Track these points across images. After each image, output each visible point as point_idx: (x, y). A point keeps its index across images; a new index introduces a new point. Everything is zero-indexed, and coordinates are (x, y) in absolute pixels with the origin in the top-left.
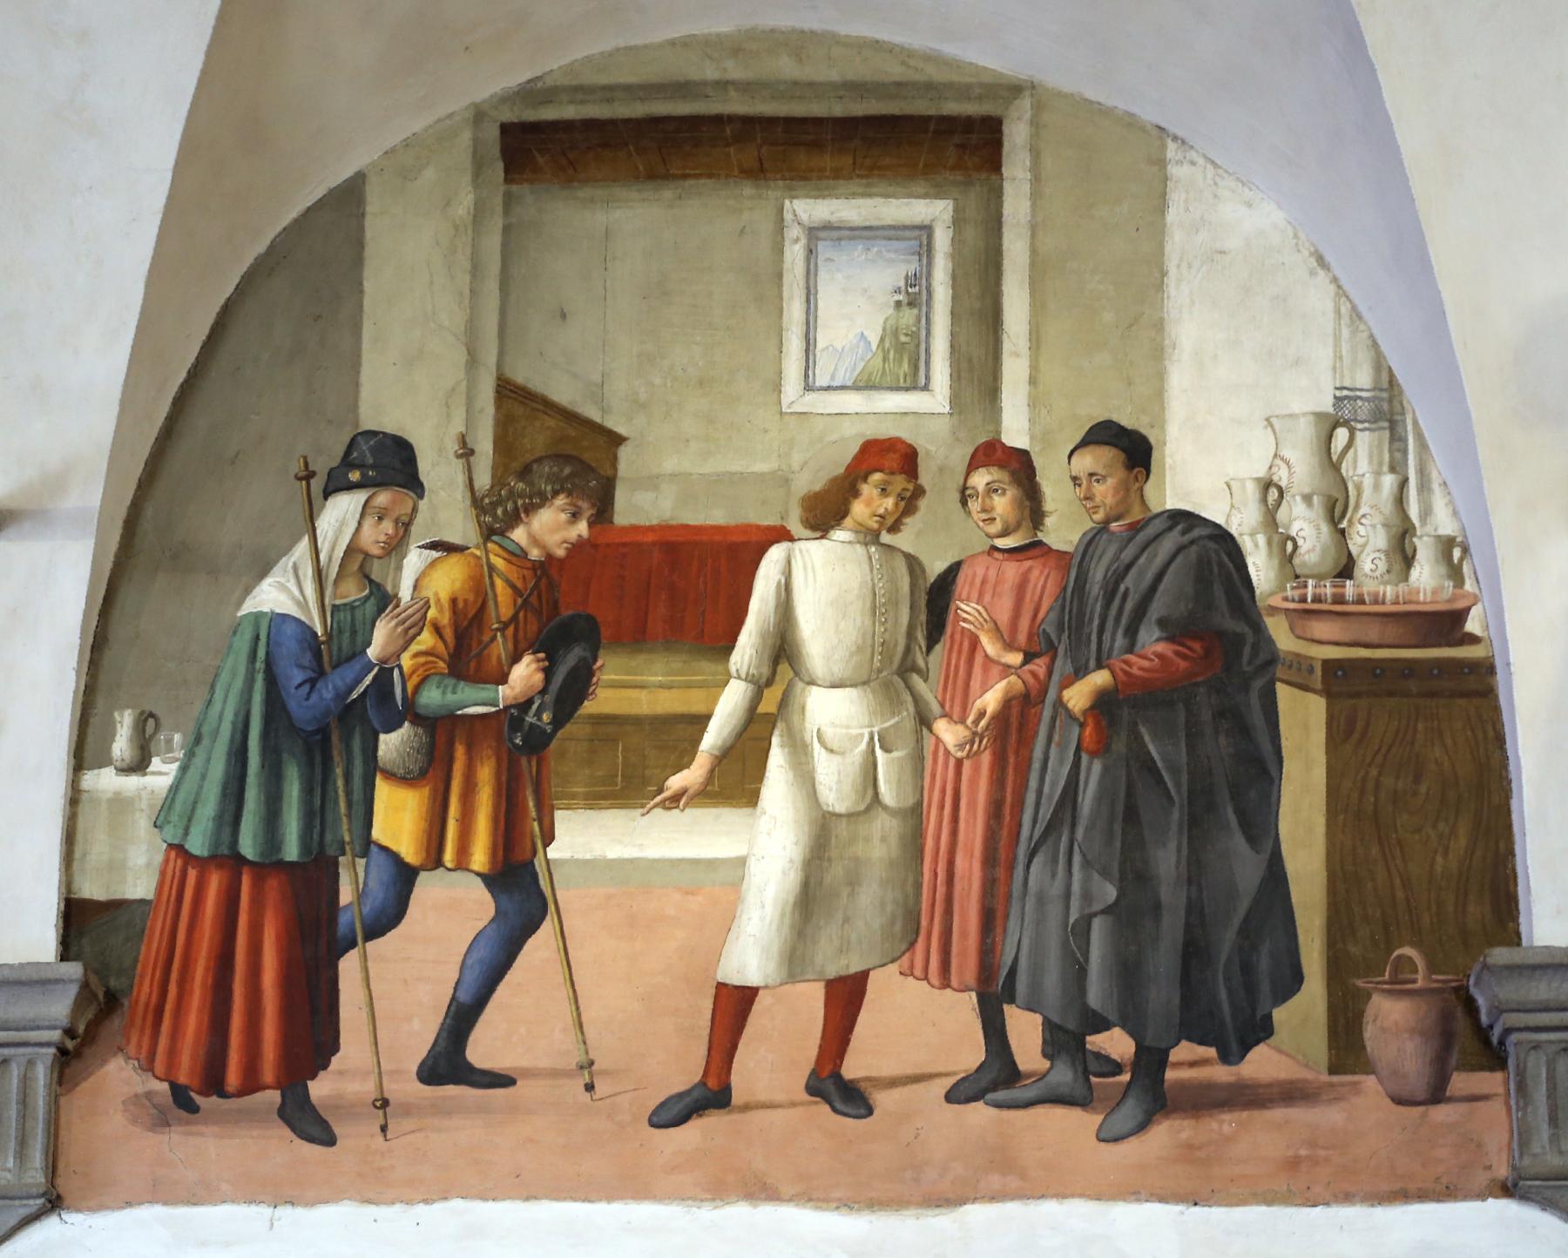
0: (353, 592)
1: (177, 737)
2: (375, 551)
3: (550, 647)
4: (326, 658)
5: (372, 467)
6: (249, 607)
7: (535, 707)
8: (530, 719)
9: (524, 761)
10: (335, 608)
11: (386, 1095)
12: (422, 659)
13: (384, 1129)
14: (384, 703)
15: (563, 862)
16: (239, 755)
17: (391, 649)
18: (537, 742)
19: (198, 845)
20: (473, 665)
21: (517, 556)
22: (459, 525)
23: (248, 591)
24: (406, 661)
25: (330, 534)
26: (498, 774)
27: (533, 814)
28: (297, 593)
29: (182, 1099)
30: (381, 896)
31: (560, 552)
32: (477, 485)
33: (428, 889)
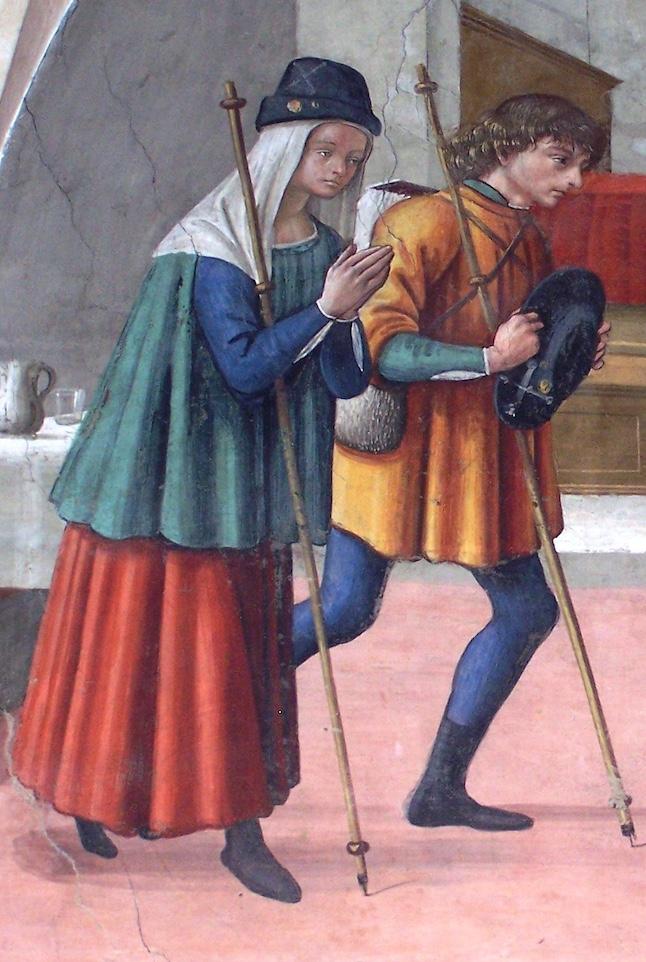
0: (297, 235)
1: (78, 396)
2: (322, 189)
3: (544, 306)
4: (265, 311)
5: (315, 97)
6: (165, 248)
7: (529, 373)
8: (524, 388)
9: (518, 436)
10: (275, 253)
11: (365, 838)
12: (385, 315)
13: (363, 880)
14: (342, 363)
15: (575, 556)
16: (159, 418)
17: (348, 301)
18: (535, 416)
19: (107, 523)
20: (449, 323)
21: (498, 201)
22: (423, 166)
23: (166, 229)
24: (367, 316)
25: (266, 170)
26: (487, 449)
27: (535, 499)
28: (228, 234)
29: (93, 840)
30: (347, 592)
31: (549, 200)
32: (443, 122)
33: (404, 587)
